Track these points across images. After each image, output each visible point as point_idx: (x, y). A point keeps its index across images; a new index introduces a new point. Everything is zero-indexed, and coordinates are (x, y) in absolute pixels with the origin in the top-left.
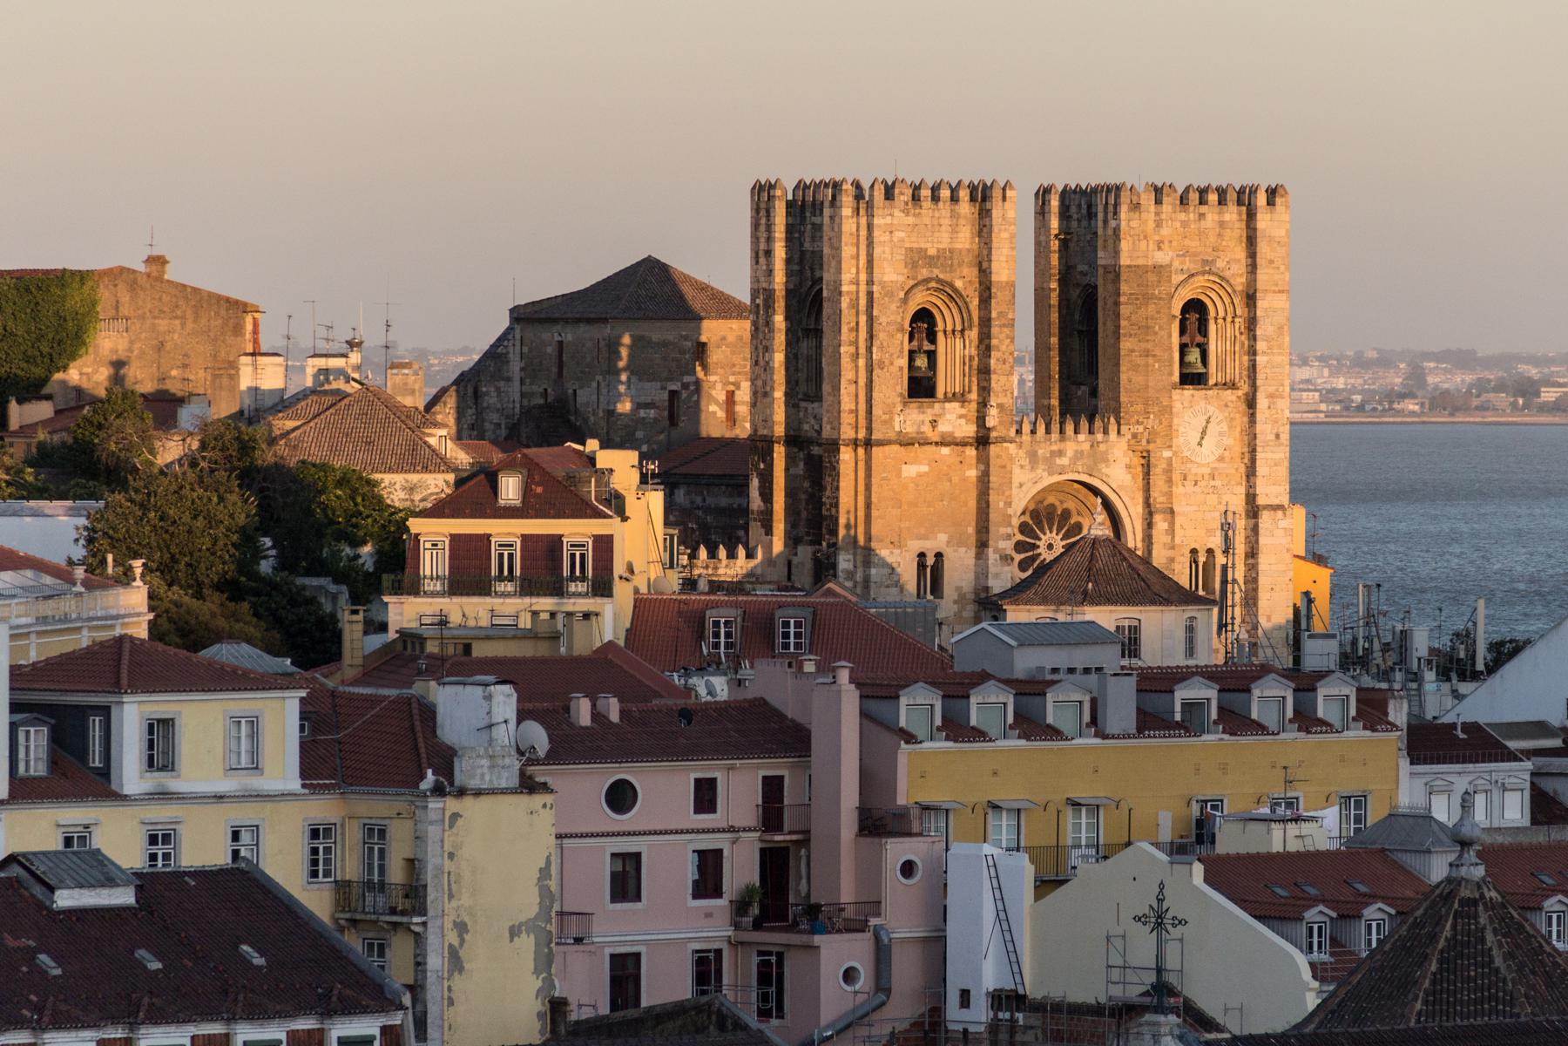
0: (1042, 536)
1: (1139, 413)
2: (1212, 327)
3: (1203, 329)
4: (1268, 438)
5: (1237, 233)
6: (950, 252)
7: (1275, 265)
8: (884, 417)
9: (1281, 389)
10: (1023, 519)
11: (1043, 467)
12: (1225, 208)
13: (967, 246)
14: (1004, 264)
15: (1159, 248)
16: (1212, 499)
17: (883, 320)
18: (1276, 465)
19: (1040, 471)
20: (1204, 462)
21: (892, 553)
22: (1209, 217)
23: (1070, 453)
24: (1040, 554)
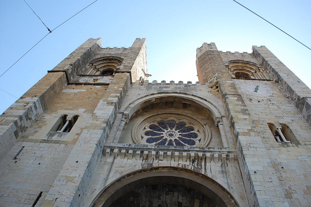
10: (152, 123)
15: (211, 48)
24: (163, 137)
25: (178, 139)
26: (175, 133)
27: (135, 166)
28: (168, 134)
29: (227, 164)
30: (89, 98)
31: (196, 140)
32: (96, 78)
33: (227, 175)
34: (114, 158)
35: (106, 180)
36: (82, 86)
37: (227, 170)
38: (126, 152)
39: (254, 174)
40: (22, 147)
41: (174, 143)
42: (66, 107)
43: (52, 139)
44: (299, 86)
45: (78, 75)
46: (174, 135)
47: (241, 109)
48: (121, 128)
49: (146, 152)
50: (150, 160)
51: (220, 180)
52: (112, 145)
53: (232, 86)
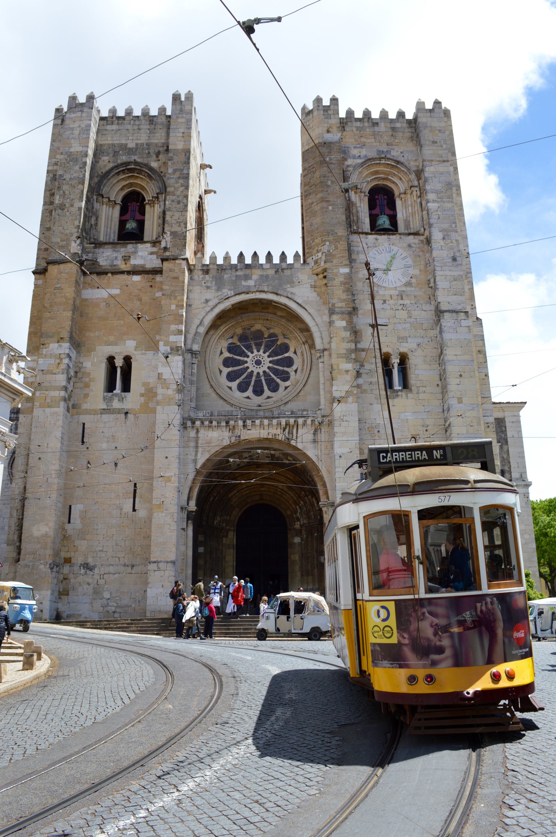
0: (249, 354)
1: (318, 245)
2: (398, 203)
3: (392, 205)
5: (408, 135)
7: (439, 144)
8: (61, 244)
10: (230, 341)
11: (229, 287)
13: (163, 141)
14: (180, 138)
15: (328, 131)
16: (403, 314)
17: (67, 177)
18: (455, 280)
19: (227, 292)
20: (392, 286)
22: (382, 125)
23: (255, 277)
24: (248, 368)
25: (267, 370)
27: (222, 440)
28: (254, 360)
29: (321, 429)
31: (292, 371)
32: (123, 251)
33: (319, 445)
34: (198, 431)
35: (195, 461)
36: (109, 278)
37: (319, 438)
39: (339, 458)
40: (82, 425)
41: (263, 379)
43: (114, 407)
45: (90, 244)
46: (263, 362)
47: (346, 350)
48: (195, 379)
49: (232, 423)
50: (236, 431)
51: (311, 453)
53: (345, 284)
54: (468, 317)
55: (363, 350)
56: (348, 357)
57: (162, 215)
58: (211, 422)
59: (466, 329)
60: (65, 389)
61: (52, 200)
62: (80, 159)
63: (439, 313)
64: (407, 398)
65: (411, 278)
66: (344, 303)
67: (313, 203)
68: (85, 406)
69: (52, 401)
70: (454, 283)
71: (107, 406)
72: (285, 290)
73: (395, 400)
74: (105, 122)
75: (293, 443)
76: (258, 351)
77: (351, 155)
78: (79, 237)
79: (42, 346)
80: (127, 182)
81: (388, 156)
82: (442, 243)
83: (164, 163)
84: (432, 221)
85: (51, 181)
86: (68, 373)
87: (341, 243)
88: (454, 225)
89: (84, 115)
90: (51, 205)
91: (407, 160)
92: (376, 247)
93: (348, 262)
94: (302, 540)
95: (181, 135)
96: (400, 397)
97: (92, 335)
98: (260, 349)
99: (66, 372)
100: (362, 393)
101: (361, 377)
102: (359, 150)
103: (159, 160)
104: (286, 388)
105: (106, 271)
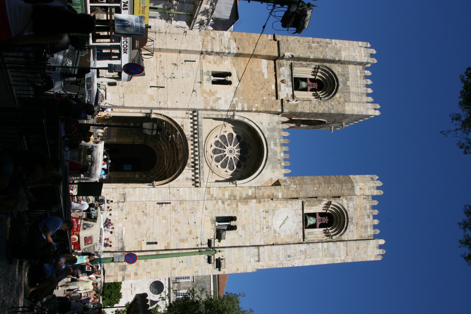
0: (235, 147)
1: (294, 182)
3: (321, 226)
4: (288, 251)
6: (349, 91)
8: (289, 47)
9: (309, 257)
10: (242, 137)
11: (269, 135)
12: (372, 228)
13: (352, 100)
15: (361, 189)
16: (258, 228)
17: (327, 49)
18: (277, 256)
20: (274, 222)
21: (235, 48)
24: (228, 146)
25: (226, 156)
26: (232, 155)
28: (232, 149)
30: (256, 85)
33: (185, 181)
34: (191, 119)
35: (176, 117)
37: (189, 181)
38: (195, 125)
42: (240, 71)
43: (204, 76)
44: (281, 254)
45: (291, 63)
46: (231, 154)
47: (236, 195)
49: (196, 136)
52: (199, 116)
53: (273, 195)
54: (256, 262)
55: (237, 206)
56: (232, 196)
57: (309, 99)
58: (196, 125)
59: (249, 261)
60: (213, 52)
61: (315, 43)
62: (337, 56)
63: (258, 246)
64: (211, 229)
65: (279, 233)
66: (261, 195)
67: (319, 179)
68: (203, 61)
69: (205, 45)
70: (275, 256)
71: (205, 73)
72: (269, 164)
73: (209, 223)
74: (362, 69)
75: (186, 167)
76: (237, 152)
77: (349, 202)
78: (293, 56)
79: (234, 39)
80: (328, 82)
81: (349, 223)
82: (298, 250)
83: (339, 101)
84: (311, 244)
85: (326, 41)
86: (221, 53)
87: (296, 194)
88: (309, 257)
89: (363, 58)
90: (313, 42)
91: (348, 234)
92: (296, 215)
93: (285, 197)
94: (137, 179)
95: (354, 109)
96: (212, 225)
97: (242, 65)
98: (238, 153)
99: (221, 51)
100: (214, 204)
101: (222, 204)
102: (353, 207)
103: (340, 98)
104: (217, 166)
105: (277, 72)
